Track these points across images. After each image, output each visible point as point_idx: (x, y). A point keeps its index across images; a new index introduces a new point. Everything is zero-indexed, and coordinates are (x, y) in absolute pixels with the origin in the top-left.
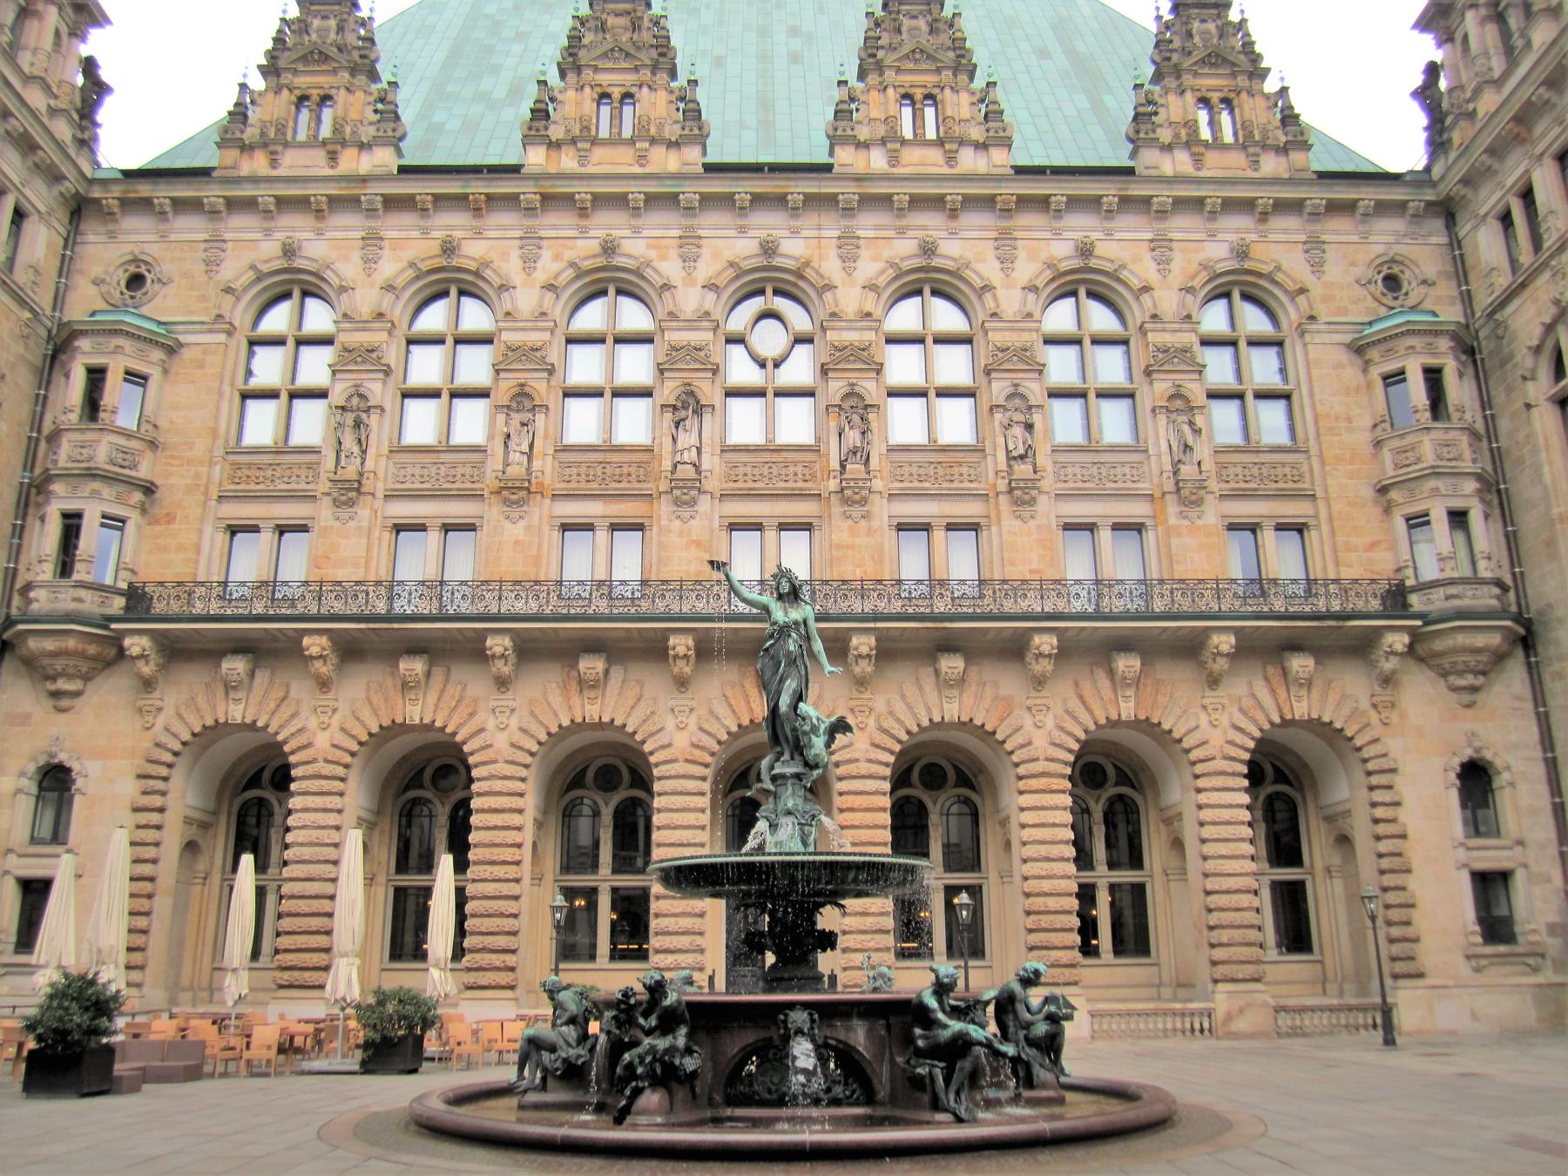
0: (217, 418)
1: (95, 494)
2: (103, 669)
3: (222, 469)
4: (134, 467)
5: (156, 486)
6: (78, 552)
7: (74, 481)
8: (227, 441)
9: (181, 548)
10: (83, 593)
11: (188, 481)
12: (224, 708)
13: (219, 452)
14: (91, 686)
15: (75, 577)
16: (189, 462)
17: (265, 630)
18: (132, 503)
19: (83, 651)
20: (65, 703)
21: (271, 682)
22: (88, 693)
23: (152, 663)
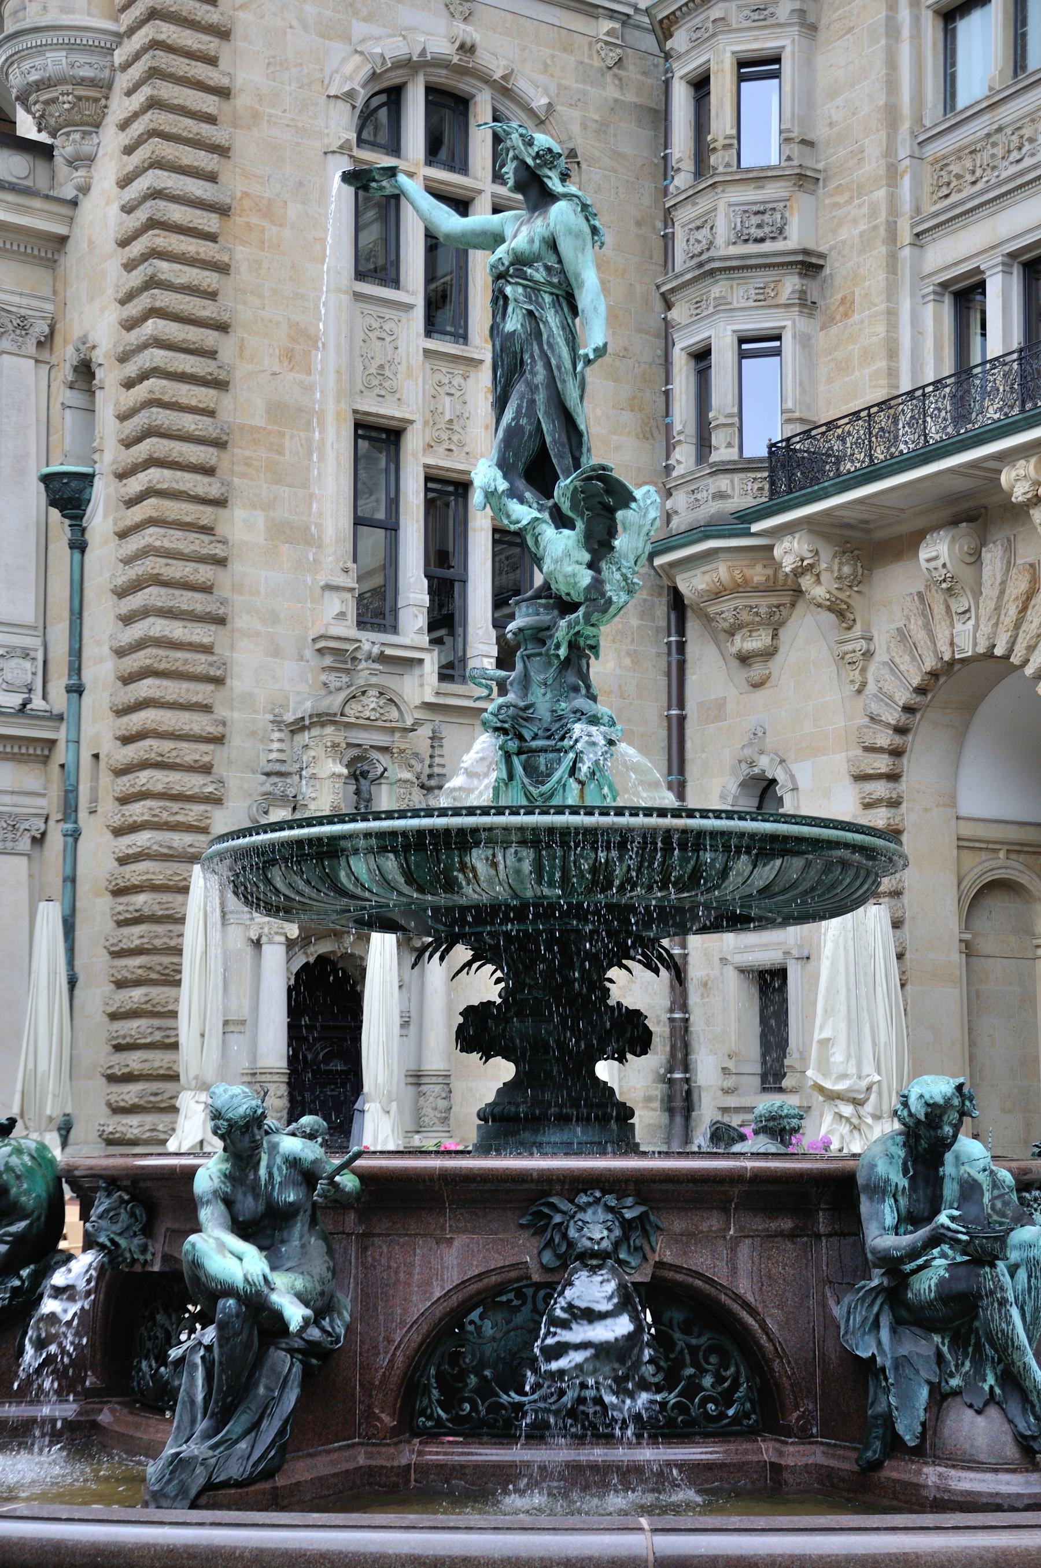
0: (891, 84)
1: (722, 306)
2: (793, 605)
3: (916, 184)
4: (781, 231)
5: (822, 256)
6: (711, 415)
7: (693, 293)
8: (918, 120)
9: (867, 356)
10: (723, 483)
11: (863, 226)
12: (947, 633)
13: (903, 152)
14: (784, 634)
15: (714, 457)
16: (861, 190)
17: (951, 470)
18: (783, 299)
19: (746, 582)
20: (757, 671)
21: (1009, 565)
22: (783, 649)
23: (825, 577)
